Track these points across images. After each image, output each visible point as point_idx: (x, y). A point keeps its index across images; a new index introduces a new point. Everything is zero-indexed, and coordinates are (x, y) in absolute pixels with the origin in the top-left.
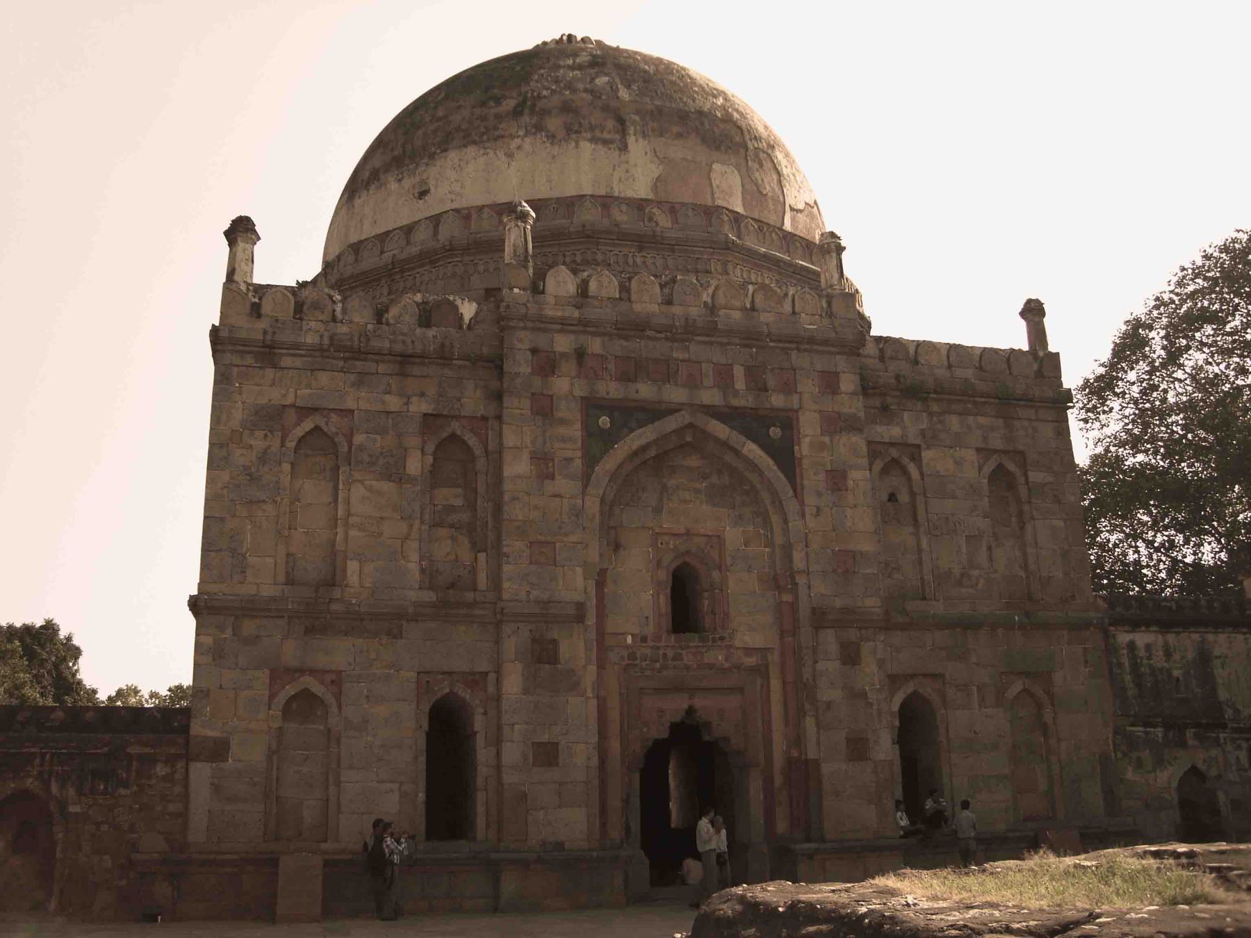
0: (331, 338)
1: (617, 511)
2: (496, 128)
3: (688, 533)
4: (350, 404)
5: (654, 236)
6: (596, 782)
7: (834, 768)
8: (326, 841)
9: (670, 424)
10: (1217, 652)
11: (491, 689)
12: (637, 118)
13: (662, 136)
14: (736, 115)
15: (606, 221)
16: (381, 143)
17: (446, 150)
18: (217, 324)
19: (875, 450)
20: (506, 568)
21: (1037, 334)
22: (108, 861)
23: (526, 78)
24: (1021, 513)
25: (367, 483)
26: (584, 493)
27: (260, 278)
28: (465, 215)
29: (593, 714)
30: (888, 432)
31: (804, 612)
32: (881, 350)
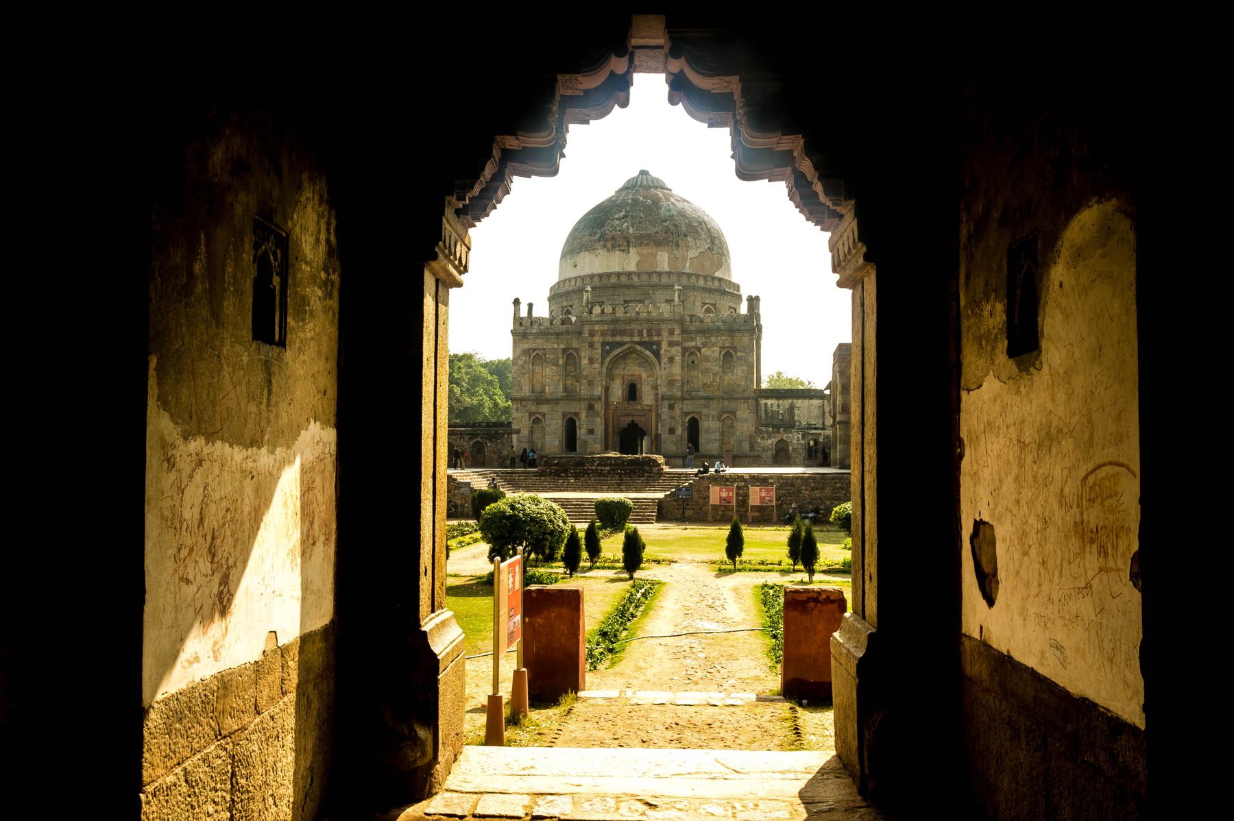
7: (665, 436)
9: (626, 347)
19: (685, 350)
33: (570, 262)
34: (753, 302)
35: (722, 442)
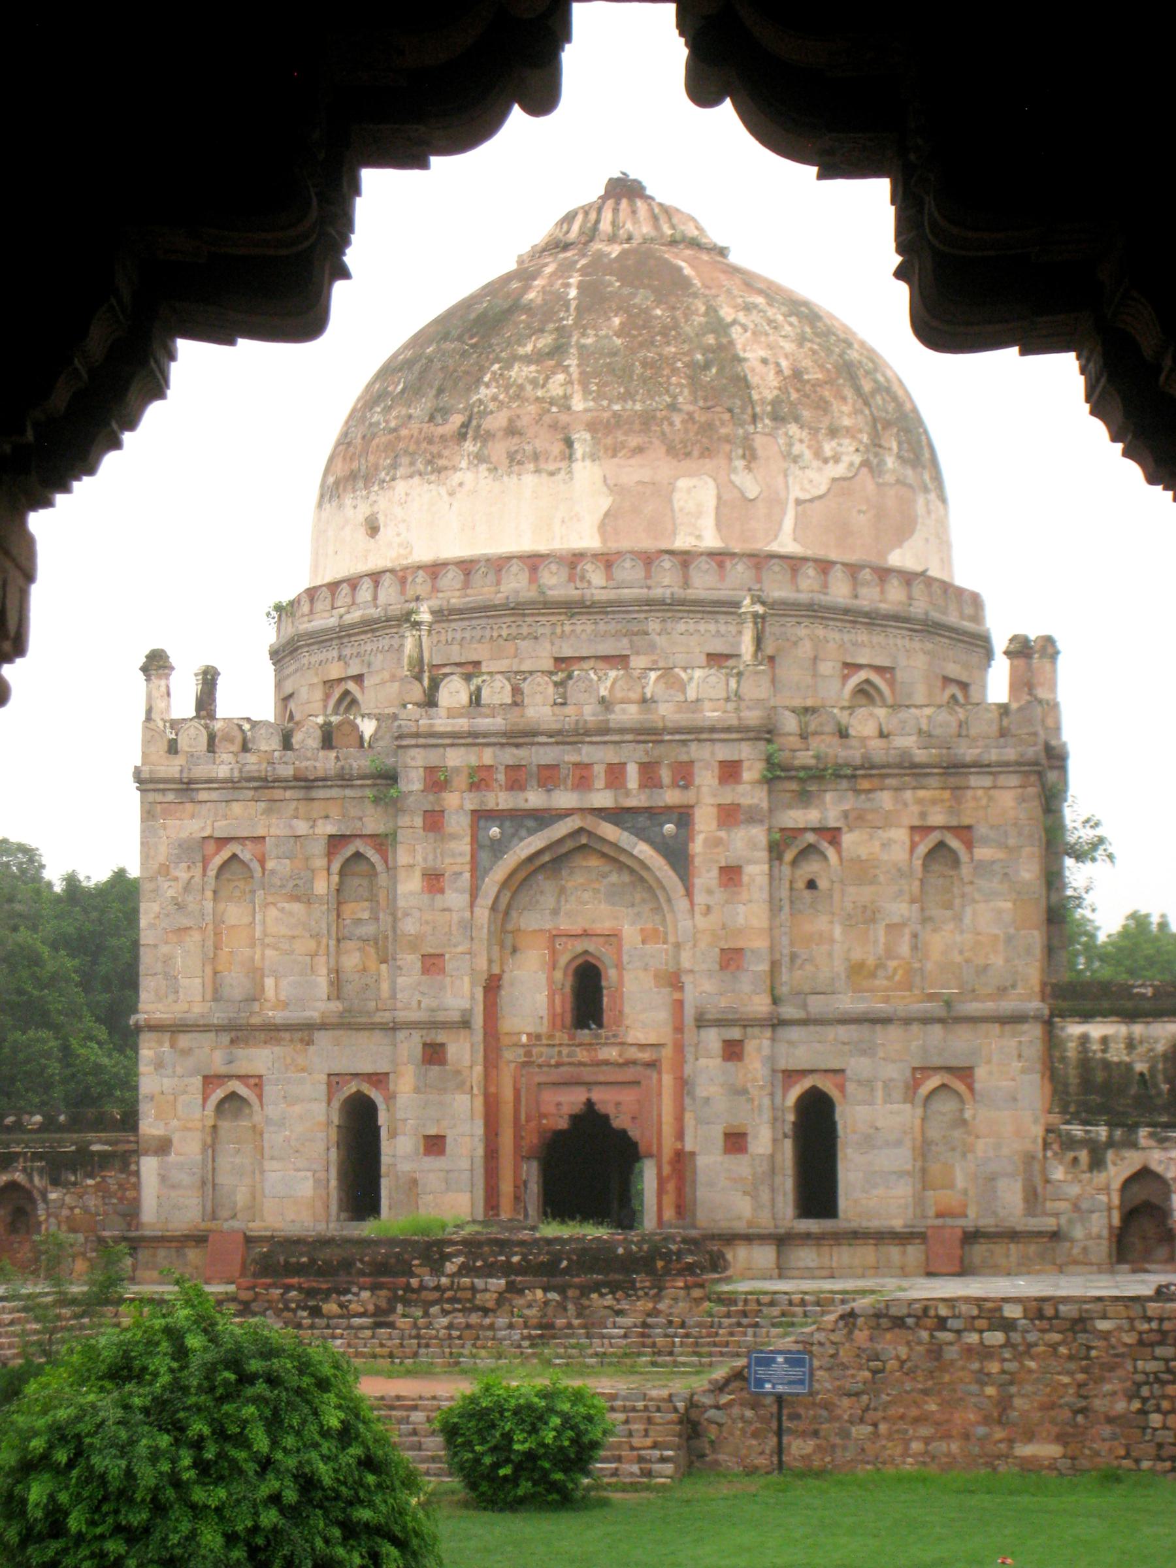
0: (241, 771)
1: (514, 914)
2: (440, 456)
3: (586, 934)
4: (260, 832)
7: (710, 1161)
11: (391, 1087)
13: (614, 456)
15: (534, 587)
18: (139, 764)
20: (400, 980)
25: (280, 905)
26: (472, 905)
27: (176, 714)
30: (796, 817)
31: (689, 1012)
33: (355, 508)
34: (1033, 655)
35: (924, 1180)
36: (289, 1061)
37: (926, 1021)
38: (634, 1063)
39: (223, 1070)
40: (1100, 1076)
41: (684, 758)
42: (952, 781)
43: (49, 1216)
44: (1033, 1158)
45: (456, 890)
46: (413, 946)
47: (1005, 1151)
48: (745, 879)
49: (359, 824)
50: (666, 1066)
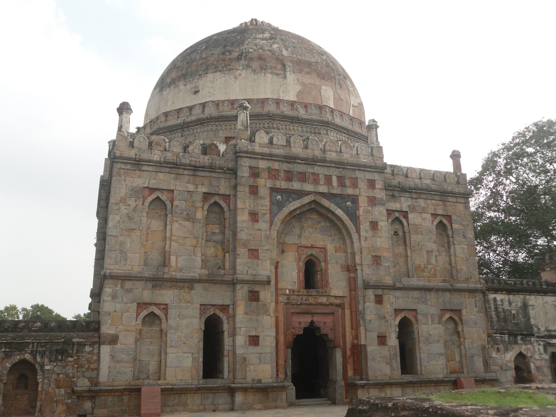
1: (283, 236)
2: (229, 65)
3: (312, 247)
5: (298, 118)
6: (275, 353)
7: (373, 348)
8: (160, 379)
9: (307, 200)
10: (530, 303)
11: (231, 311)
12: (291, 64)
14: (331, 64)
15: (278, 110)
16: (174, 66)
17: (207, 73)
19: (390, 212)
20: (239, 261)
21: (457, 166)
22: (62, 391)
23: (242, 43)
24: (449, 242)
28: (217, 104)
29: (274, 323)
30: (394, 206)
32: (393, 171)
36: (181, 297)
37: (444, 290)
38: (332, 304)
39: (147, 300)
40: (502, 315)
41: (354, 176)
42: (443, 198)
43: (44, 378)
44: (485, 348)
45: (264, 221)
46: (245, 245)
47: (475, 345)
48: (379, 227)
49: (217, 189)
50: (347, 306)
